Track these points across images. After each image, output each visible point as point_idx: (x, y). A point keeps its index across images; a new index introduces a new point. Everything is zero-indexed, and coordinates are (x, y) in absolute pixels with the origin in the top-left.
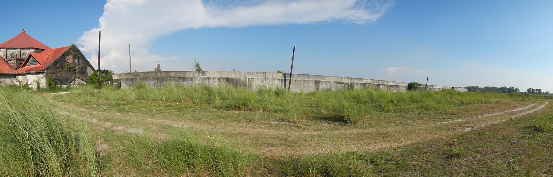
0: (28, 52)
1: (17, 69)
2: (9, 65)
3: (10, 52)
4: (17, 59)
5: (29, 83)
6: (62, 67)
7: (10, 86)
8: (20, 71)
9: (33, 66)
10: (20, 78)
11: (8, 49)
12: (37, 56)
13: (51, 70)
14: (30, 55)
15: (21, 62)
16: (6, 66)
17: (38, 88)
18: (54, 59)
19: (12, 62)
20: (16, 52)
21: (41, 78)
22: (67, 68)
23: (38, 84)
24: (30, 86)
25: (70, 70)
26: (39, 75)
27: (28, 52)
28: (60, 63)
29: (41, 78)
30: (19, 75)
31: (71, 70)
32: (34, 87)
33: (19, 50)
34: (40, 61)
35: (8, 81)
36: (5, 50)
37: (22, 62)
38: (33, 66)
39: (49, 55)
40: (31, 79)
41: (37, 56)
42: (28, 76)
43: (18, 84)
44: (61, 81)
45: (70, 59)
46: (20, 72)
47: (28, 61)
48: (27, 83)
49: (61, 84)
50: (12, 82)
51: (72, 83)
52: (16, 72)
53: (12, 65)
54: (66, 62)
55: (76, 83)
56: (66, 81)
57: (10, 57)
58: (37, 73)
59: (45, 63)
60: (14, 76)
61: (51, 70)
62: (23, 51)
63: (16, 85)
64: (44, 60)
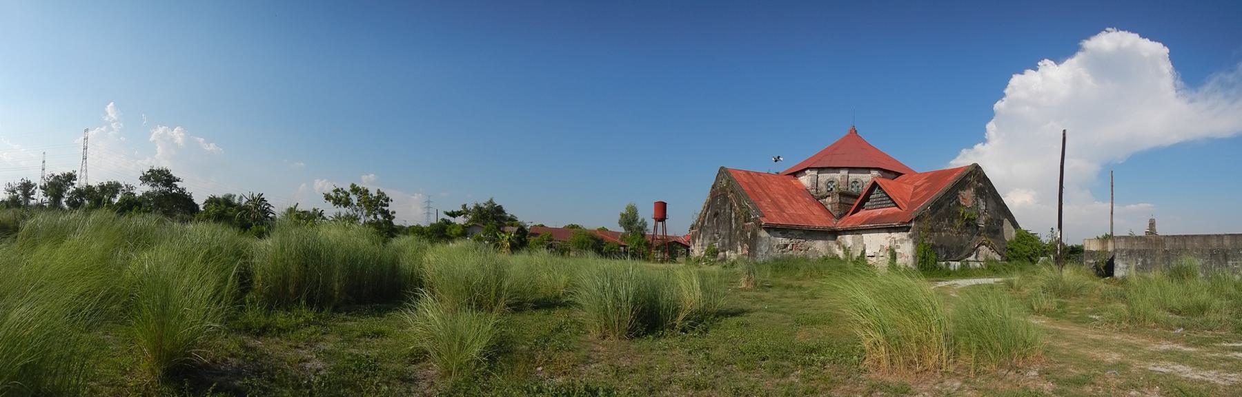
0: (867, 178)
1: (840, 217)
2: (823, 207)
3: (824, 177)
4: (842, 194)
5: (868, 252)
6: (952, 215)
7: (825, 258)
8: (848, 222)
9: (879, 212)
10: (848, 239)
11: (821, 170)
12: (888, 184)
13: (926, 224)
14: (874, 185)
15: (851, 200)
16: (816, 210)
18: (933, 197)
19: (829, 200)
20: (838, 176)
21: (902, 241)
22: (961, 217)
23: (894, 256)
24: (871, 261)
25: (967, 225)
26: (897, 236)
27: (867, 178)
28: (945, 207)
29: (902, 241)
31: (970, 224)
32: (882, 262)
33: (844, 173)
34: (898, 201)
35: (820, 246)
36: (815, 173)
37: (851, 201)
38: (879, 212)
39: (916, 188)
40: (875, 243)
41: (888, 184)
42: (866, 236)
43: (841, 253)
44: (948, 252)
45: (967, 196)
46: (849, 226)
47: (867, 198)
48: (863, 252)
49: (949, 258)
50: (829, 248)
51: (972, 258)
52: (839, 225)
53: (829, 207)
54: (958, 204)
55: (981, 258)
56: (958, 251)
57: (824, 189)
58: (890, 230)
59: (911, 205)
60: (833, 234)
61: (926, 224)
62: (853, 176)
63: (836, 258)
64: (908, 198)
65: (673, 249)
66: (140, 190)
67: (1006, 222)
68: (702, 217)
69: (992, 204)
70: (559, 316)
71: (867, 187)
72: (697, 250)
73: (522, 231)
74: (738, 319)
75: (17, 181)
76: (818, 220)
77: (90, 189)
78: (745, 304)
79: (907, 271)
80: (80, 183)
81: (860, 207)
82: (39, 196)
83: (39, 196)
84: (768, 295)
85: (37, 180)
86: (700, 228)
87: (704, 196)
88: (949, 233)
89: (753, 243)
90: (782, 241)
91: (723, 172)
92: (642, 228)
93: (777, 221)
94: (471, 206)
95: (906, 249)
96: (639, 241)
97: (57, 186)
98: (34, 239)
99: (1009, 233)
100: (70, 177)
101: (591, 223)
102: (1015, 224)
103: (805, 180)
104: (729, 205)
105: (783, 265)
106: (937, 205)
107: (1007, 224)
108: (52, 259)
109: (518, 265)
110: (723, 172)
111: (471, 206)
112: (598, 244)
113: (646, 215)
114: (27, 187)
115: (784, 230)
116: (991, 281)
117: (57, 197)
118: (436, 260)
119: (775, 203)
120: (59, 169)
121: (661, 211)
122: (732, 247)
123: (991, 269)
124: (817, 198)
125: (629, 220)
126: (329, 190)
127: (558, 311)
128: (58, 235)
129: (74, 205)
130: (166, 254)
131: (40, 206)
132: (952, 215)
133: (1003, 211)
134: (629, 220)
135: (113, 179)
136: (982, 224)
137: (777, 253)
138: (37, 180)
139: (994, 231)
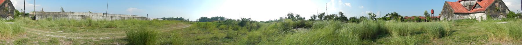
6: (494, 9)
10: (472, 15)
17: (482, 20)
23: (482, 18)
30: (471, 13)
31: (498, 10)
32: (480, 20)
35: (466, 17)
37: (472, 7)
40: (478, 16)
43: (470, 18)
52: (470, 12)
56: (496, 16)
58: (481, 12)
59: (485, 7)
60: (469, 14)
65: (436, 19)
66: (339, 16)
67: (507, 10)
68: (442, 12)
69: (503, 6)
70: (422, 36)
71: (474, 5)
72: (442, 19)
73: (402, 18)
74: (455, 33)
75: (312, 15)
76: (465, 11)
77: (328, 16)
78: (455, 29)
79: (485, 21)
80: (326, 15)
81: (474, 8)
82: (317, 18)
83: (317, 18)
84: (459, 27)
85: (317, 15)
86: (442, 14)
87: (442, 8)
88: (494, 13)
89: (452, 16)
90: (458, 16)
91: (446, 2)
92: (429, 15)
93: (457, 12)
94: (390, 13)
95: (484, 16)
96: (427, 18)
97: (321, 16)
98: (316, 28)
99: (507, 12)
100: (324, 14)
101: (418, 15)
102: (508, 10)
103: (462, 3)
104: (447, 9)
105: (458, 21)
106: (491, 7)
107: (507, 10)
108: (322, 32)
109: (411, 25)
110: (446, 2)
111: (390, 13)
112: (419, 20)
113: (429, 12)
114: (315, 16)
115: (458, 14)
116: (505, 22)
117: (321, 18)
118: (390, 24)
119: (456, 8)
120: (321, 12)
121: (433, 12)
122: (449, 18)
123: (503, 20)
124: (465, 7)
125: (426, 14)
126: (369, 12)
127: (421, 35)
128: (322, 27)
129: (325, 19)
130: (346, 30)
131: (318, 20)
132: (494, 9)
133: (505, 7)
134: (426, 14)
135: (333, 13)
136: (501, 10)
137: (457, 19)
138: (317, 15)
139: (504, 12)
